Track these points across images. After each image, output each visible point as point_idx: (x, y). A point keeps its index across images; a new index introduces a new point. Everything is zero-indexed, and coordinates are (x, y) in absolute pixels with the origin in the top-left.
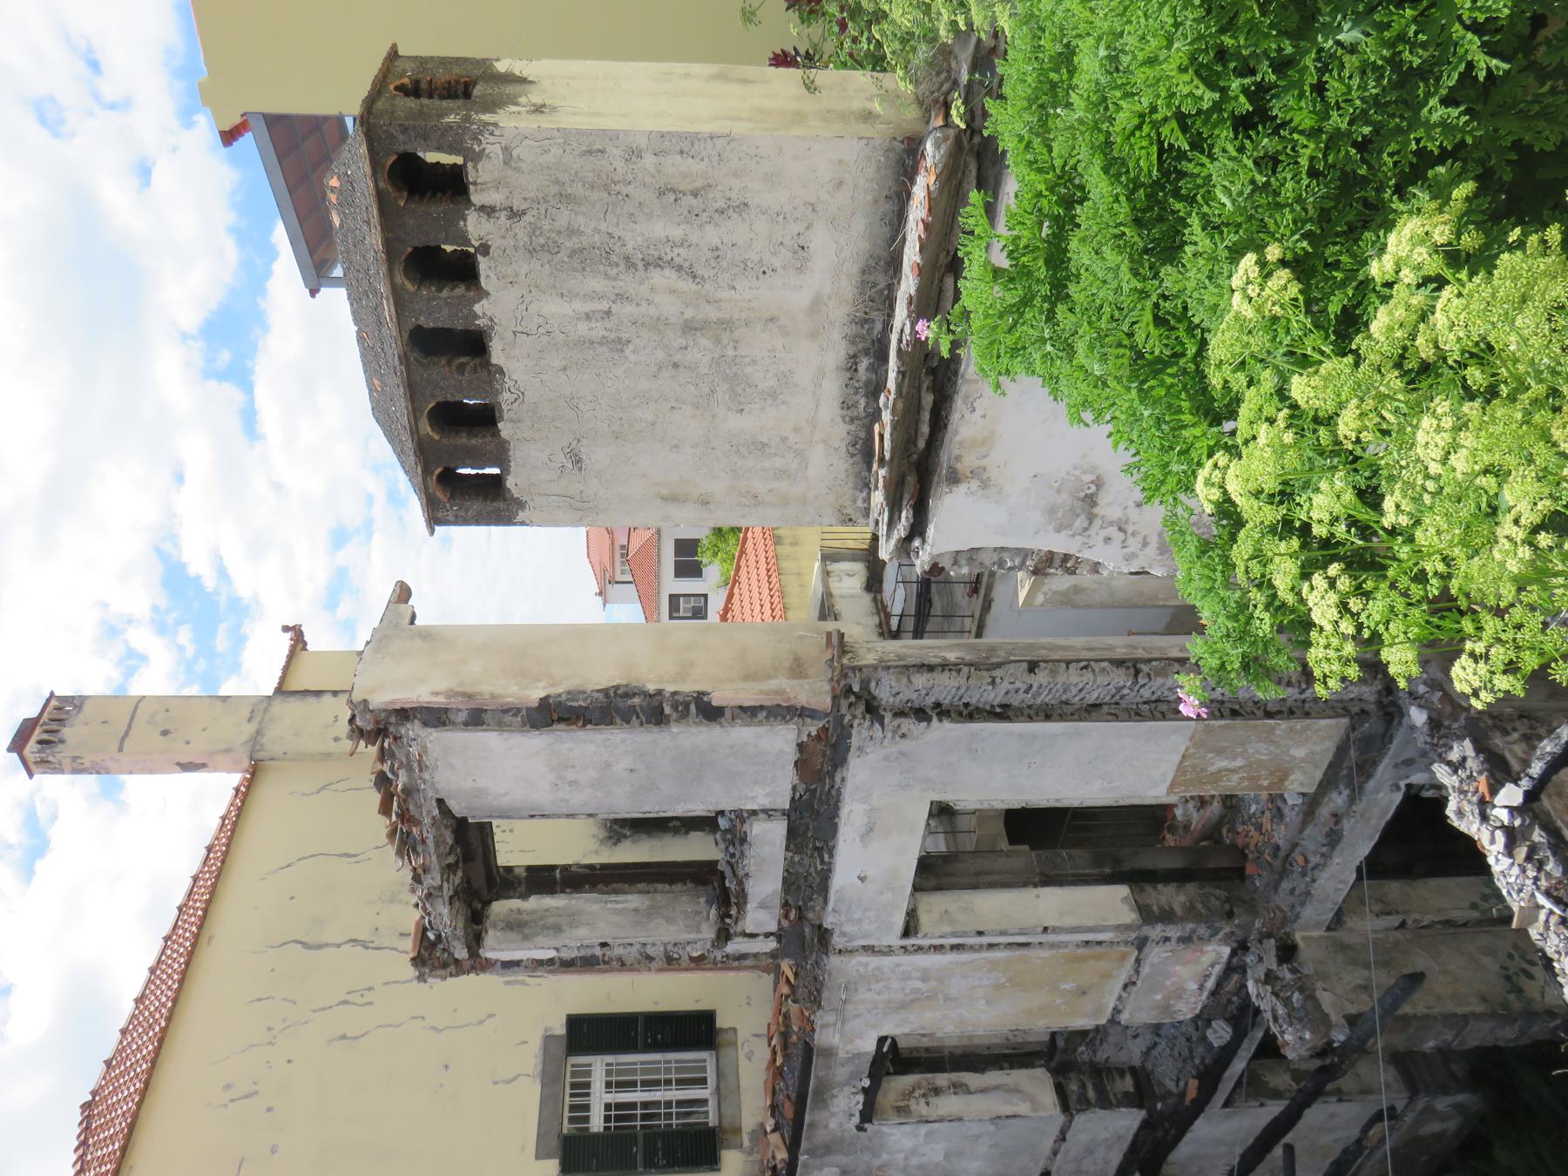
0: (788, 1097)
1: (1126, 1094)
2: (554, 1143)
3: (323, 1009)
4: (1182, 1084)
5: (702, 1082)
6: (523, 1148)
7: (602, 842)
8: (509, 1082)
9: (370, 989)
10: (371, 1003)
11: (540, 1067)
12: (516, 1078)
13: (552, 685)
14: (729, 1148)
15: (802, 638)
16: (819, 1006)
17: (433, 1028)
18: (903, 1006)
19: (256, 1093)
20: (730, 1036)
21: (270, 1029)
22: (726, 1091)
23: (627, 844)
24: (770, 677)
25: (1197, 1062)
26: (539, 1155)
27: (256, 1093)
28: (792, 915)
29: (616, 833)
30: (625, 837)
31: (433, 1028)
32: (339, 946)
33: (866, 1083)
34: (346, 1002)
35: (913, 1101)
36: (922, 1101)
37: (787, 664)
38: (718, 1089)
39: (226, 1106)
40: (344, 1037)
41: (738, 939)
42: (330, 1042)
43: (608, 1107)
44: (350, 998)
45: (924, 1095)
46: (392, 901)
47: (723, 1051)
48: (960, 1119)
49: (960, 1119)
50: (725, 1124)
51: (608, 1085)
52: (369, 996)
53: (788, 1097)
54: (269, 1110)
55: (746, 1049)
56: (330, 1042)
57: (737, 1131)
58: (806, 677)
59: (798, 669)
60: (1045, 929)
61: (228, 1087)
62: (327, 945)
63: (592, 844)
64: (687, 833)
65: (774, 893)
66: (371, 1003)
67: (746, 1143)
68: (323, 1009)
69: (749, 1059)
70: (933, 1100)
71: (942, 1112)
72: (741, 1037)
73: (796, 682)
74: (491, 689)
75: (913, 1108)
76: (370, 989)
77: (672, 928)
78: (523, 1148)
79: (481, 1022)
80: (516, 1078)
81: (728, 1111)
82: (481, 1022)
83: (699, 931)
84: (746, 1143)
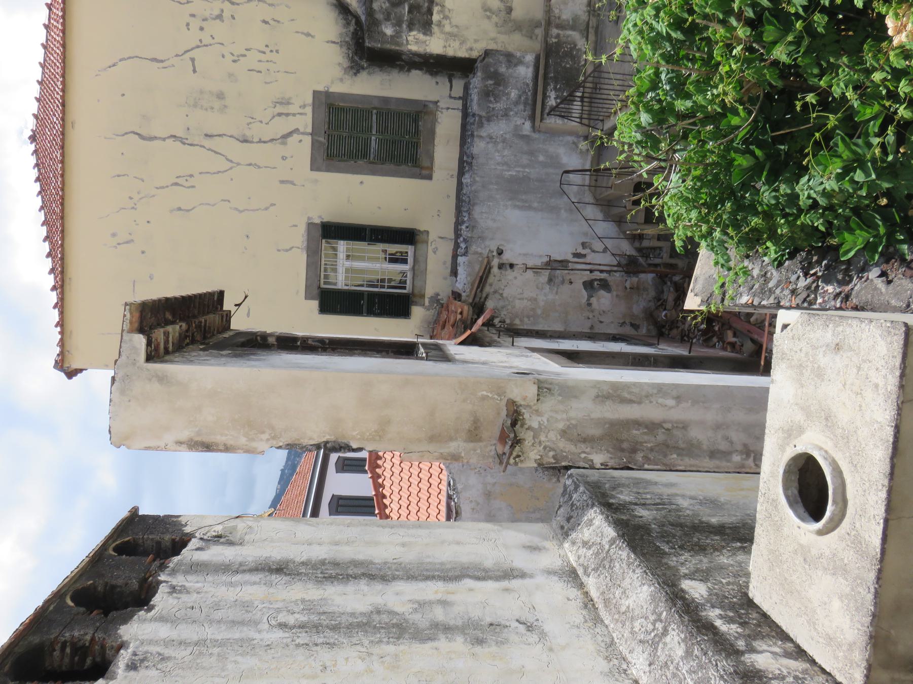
2: (316, 292)
3: (163, 188)
5: (405, 261)
6: (298, 292)
7: (346, 70)
8: (287, 251)
9: (191, 176)
10: (193, 187)
11: (305, 244)
12: (291, 248)
13: (274, 438)
14: (416, 304)
15: (484, 398)
17: (236, 209)
19: (132, 241)
20: (424, 237)
21: (131, 198)
22: (419, 270)
23: (364, 75)
24: (451, 439)
26: (308, 297)
27: (132, 241)
29: (357, 64)
30: (363, 68)
31: (236, 209)
32: (164, 139)
34: (176, 184)
37: (467, 426)
38: (413, 269)
39: (116, 247)
40: (179, 209)
42: (171, 211)
43: (347, 271)
44: (178, 181)
46: (195, 106)
47: (419, 246)
50: (416, 291)
51: (348, 257)
52: (191, 182)
54: (143, 252)
55: (433, 246)
56: (171, 211)
57: (423, 296)
58: (480, 440)
59: (474, 434)
61: (114, 235)
62: (156, 138)
63: (338, 72)
64: (409, 71)
66: (193, 187)
68: (163, 188)
69: (435, 252)
72: (432, 237)
73: (471, 445)
74: (224, 438)
76: (191, 176)
78: (298, 292)
79: (266, 209)
80: (291, 248)
81: (418, 283)
82: (266, 209)
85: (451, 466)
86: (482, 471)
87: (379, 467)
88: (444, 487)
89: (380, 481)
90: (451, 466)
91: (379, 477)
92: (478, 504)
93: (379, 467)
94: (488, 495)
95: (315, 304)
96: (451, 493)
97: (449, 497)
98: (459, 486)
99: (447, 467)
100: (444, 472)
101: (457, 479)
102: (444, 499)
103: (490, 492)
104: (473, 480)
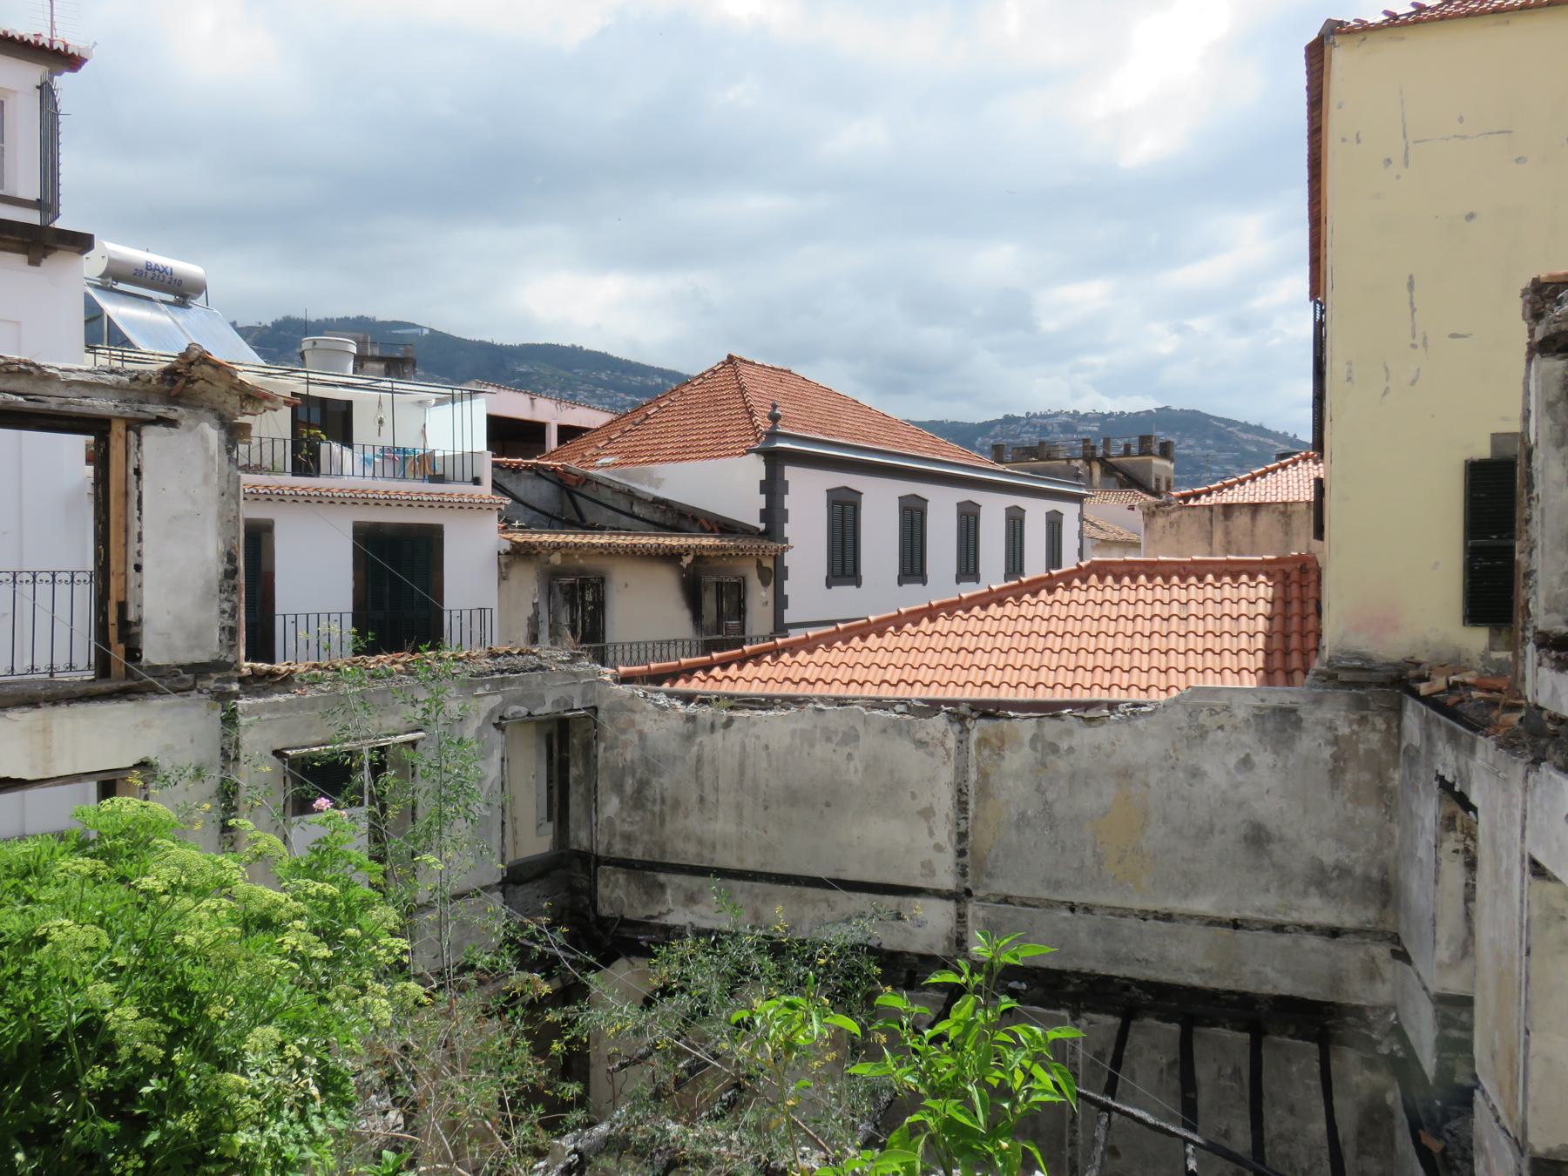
0: (1462, 701)
1: (1453, 1072)
2: (1508, 452)
4: (1447, 1136)
6: (1505, 419)
14: (1491, 635)
16: (1500, 746)
18: (1493, 841)
25: (1458, 1162)
28: (1551, 727)
33: (1457, 789)
35: (1461, 836)
36: (1461, 847)
41: (1536, 657)
45: (1467, 850)
48: (1436, 882)
49: (1436, 882)
53: (1462, 701)
60: (1528, 1032)
65: (1561, 706)
67: (1495, 655)
70: (1460, 859)
71: (1444, 864)
75: (1452, 835)
77: (1556, 580)
78: (1505, 419)
83: (1548, 611)
84: (1495, 655)
85: (1179, 707)
86: (1170, 762)
87: (1101, 579)
88: (1135, 695)
89: (1077, 582)
90: (1179, 707)
91: (1084, 580)
92: (1109, 757)
93: (1101, 579)
94: (1125, 774)
95: (1483, 451)
96: (1121, 708)
97: (1112, 706)
98: (1140, 723)
99: (1176, 700)
100: (1163, 696)
101: (1153, 718)
102: (1116, 695)
103: (1131, 777)
104: (1153, 747)
